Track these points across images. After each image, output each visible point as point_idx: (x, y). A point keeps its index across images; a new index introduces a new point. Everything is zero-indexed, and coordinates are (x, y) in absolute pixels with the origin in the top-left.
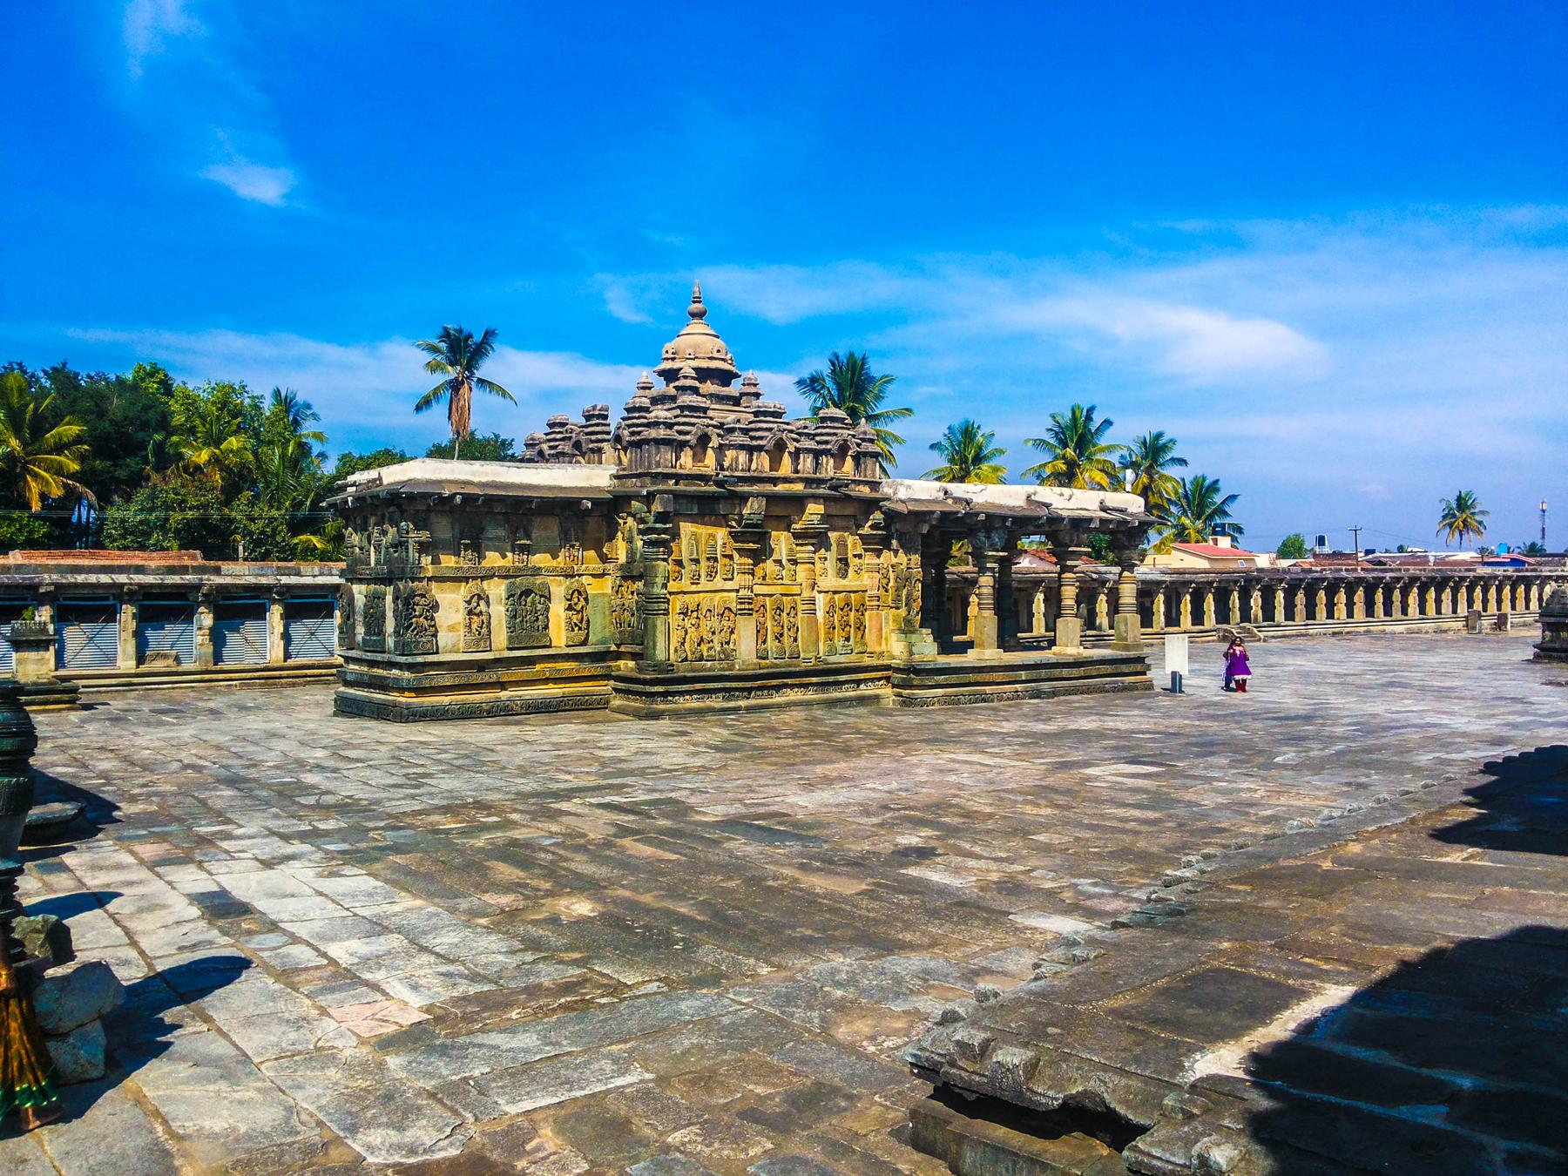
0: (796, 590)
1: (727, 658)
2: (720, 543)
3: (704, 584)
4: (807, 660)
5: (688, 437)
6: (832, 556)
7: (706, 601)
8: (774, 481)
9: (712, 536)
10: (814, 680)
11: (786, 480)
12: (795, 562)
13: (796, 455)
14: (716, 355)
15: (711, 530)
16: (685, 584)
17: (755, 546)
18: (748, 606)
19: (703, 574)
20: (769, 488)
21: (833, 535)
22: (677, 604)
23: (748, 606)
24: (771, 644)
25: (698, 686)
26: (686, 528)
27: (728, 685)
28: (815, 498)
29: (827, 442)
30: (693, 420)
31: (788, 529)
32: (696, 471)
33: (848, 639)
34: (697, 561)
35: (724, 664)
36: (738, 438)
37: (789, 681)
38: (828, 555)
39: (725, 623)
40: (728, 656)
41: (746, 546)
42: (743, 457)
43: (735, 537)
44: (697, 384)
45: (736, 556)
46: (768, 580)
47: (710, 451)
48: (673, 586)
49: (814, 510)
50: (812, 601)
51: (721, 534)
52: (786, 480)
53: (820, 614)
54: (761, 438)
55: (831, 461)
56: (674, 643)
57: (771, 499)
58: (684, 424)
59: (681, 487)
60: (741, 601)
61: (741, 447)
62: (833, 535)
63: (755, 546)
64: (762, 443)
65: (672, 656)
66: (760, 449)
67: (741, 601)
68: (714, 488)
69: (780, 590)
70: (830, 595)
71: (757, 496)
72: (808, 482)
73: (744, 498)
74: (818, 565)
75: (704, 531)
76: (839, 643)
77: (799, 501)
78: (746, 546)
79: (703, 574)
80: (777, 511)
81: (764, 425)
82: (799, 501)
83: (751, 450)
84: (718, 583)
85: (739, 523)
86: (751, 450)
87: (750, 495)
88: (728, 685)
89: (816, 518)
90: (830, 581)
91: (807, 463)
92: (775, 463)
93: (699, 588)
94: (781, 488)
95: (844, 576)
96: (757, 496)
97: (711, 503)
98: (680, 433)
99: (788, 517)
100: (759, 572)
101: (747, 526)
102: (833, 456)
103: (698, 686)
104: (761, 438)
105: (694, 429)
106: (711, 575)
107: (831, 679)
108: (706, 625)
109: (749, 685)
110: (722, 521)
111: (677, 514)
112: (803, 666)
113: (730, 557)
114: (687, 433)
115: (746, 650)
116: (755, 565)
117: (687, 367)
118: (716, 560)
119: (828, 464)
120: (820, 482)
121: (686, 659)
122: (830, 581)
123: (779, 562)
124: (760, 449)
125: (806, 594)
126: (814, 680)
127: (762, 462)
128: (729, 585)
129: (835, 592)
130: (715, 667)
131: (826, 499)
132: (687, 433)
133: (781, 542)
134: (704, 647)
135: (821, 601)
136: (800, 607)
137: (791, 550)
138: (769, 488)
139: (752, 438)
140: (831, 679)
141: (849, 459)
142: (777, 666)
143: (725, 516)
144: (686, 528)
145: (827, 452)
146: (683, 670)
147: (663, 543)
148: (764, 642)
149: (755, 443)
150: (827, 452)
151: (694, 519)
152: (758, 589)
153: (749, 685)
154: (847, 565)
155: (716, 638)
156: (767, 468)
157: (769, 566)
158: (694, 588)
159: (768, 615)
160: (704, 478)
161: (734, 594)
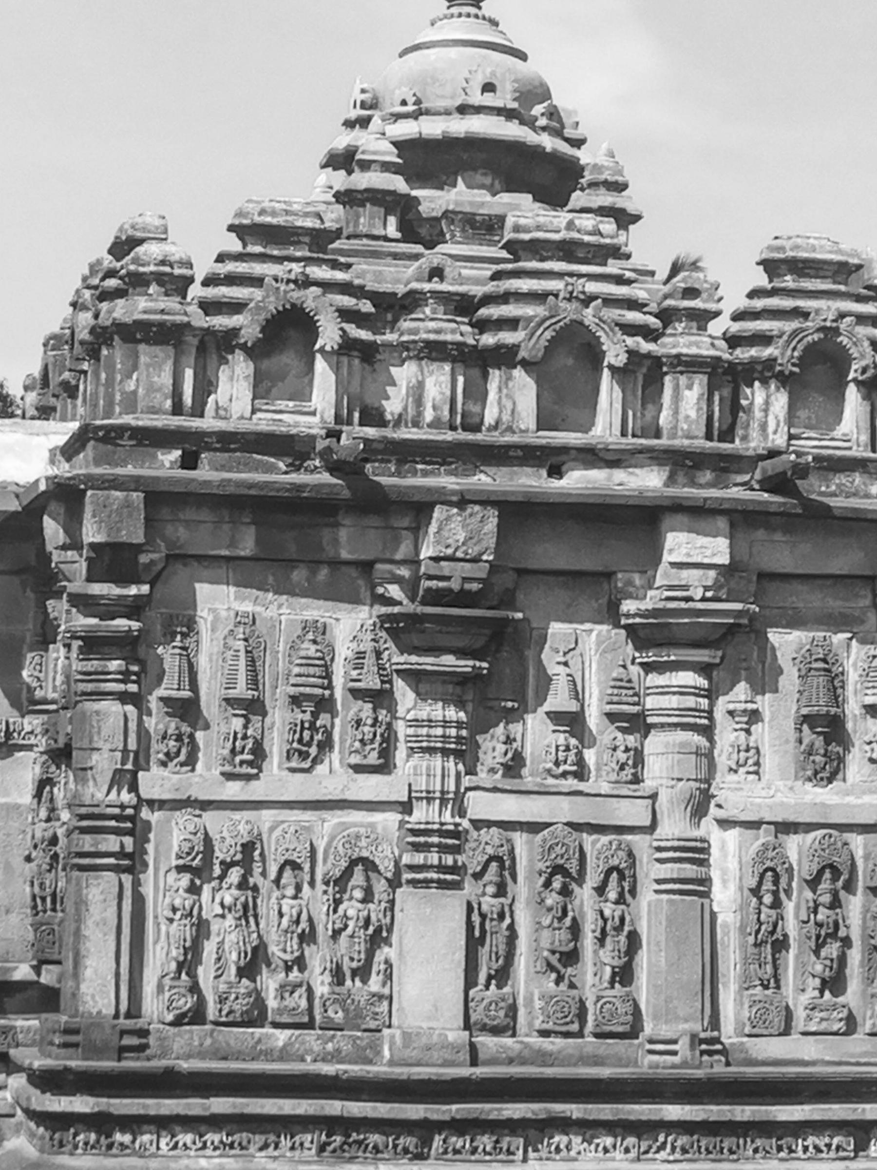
0: (633, 813)
1: (354, 1019)
2: (344, 651)
3: (277, 779)
4: (668, 1038)
5: (235, 321)
6: (780, 710)
7: (280, 835)
8: (554, 461)
9: (319, 631)
10: (674, 1112)
11: (593, 456)
12: (637, 723)
13: (646, 376)
14: (477, 98)
15: (315, 610)
16: (206, 779)
17: (465, 665)
18: (444, 856)
19: (276, 746)
20: (531, 481)
21: (787, 642)
22: (172, 835)
23: (444, 856)
24: (528, 982)
25: (220, 1105)
26: (217, 603)
27: (334, 1107)
28: (698, 514)
29: (765, 339)
30: (258, 269)
31: (611, 614)
32: (263, 422)
33: (834, 983)
34: (253, 707)
35: (341, 1041)
36: (430, 324)
37: (575, 1110)
38: (765, 703)
39: (351, 908)
40: (365, 1022)
41: (427, 662)
42: (439, 383)
43: (400, 629)
44: (398, 184)
45: (405, 695)
46: (529, 780)
47: (320, 364)
48: (156, 782)
49: (692, 554)
50: (697, 853)
51: (350, 626)
52: (593, 456)
53: (726, 897)
54: (512, 323)
55: (780, 401)
56: (160, 957)
57: (517, 513)
58: (231, 280)
59: (207, 472)
60: (418, 838)
61: (434, 351)
62: (787, 642)
63: (465, 665)
64: (508, 337)
65: (153, 1006)
66: (505, 357)
67: (418, 838)
68: (326, 478)
69: (558, 810)
70: (765, 836)
71: (463, 501)
72: (682, 463)
73: (420, 509)
74: (727, 736)
75: (283, 613)
76: (799, 990)
77: (639, 524)
78: (427, 662)
79: (276, 746)
80: (552, 553)
81: (525, 285)
82: (639, 524)
83: (476, 362)
84: (332, 778)
85: (411, 587)
86: (476, 362)
87: (442, 498)
88: (334, 1107)
89: (697, 582)
90: (775, 787)
91: (685, 407)
92: (565, 400)
93: (256, 790)
94: (577, 481)
95: (830, 770)
96: (463, 501)
97: (311, 523)
98: (209, 307)
99: (609, 575)
100: (492, 749)
101: (435, 597)
102: (784, 380)
103: (220, 1105)
104: (512, 323)
105: (257, 294)
106: (310, 747)
107: (744, 1112)
108: (276, 909)
109: (415, 1111)
110: (351, 581)
111: (178, 558)
112: (647, 1064)
113: (381, 698)
114: (237, 307)
115: (424, 991)
116: (480, 725)
117: (375, 143)
118: (324, 704)
119: (769, 413)
120: (726, 465)
121: (197, 1016)
122: (775, 787)
123: (572, 722)
124: (505, 357)
125: (674, 826)
126: (674, 1112)
127: (513, 402)
128: (371, 787)
129: (786, 828)
130: (313, 1053)
131: (741, 520)
132: (237, 307)
133: (582, 656)
134: (270, 983)
135: (730, 859)
136: (650, 870)
137: (623, 684)
138: (531, 481)
139: (482, 326)
140: (744, 1112)
141: (852, 394)
142: (543, 1058)
143: (366, 567)
144: (217, 603)
145: (763, 372)
146: (184, 1050)
147: (128, 646)
148: (502, 976)
149: (488, 339)
150: (763, 372)
151: (244, 572)
152: (481, 806)
153: (415, 1111)
154: (845, 742)
155: (317, 959)
156: (527, 418)
157: (537, 734)
158: (233, 790)
159: (523, 889)
160: (291, 448)
161: (390, 820)
